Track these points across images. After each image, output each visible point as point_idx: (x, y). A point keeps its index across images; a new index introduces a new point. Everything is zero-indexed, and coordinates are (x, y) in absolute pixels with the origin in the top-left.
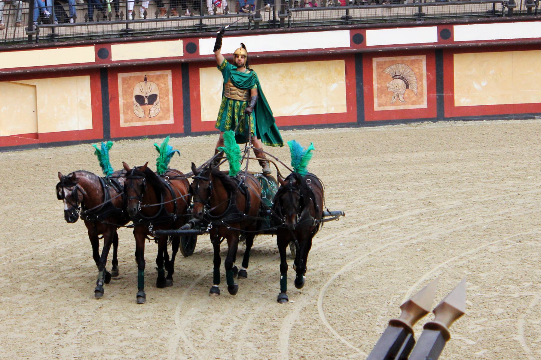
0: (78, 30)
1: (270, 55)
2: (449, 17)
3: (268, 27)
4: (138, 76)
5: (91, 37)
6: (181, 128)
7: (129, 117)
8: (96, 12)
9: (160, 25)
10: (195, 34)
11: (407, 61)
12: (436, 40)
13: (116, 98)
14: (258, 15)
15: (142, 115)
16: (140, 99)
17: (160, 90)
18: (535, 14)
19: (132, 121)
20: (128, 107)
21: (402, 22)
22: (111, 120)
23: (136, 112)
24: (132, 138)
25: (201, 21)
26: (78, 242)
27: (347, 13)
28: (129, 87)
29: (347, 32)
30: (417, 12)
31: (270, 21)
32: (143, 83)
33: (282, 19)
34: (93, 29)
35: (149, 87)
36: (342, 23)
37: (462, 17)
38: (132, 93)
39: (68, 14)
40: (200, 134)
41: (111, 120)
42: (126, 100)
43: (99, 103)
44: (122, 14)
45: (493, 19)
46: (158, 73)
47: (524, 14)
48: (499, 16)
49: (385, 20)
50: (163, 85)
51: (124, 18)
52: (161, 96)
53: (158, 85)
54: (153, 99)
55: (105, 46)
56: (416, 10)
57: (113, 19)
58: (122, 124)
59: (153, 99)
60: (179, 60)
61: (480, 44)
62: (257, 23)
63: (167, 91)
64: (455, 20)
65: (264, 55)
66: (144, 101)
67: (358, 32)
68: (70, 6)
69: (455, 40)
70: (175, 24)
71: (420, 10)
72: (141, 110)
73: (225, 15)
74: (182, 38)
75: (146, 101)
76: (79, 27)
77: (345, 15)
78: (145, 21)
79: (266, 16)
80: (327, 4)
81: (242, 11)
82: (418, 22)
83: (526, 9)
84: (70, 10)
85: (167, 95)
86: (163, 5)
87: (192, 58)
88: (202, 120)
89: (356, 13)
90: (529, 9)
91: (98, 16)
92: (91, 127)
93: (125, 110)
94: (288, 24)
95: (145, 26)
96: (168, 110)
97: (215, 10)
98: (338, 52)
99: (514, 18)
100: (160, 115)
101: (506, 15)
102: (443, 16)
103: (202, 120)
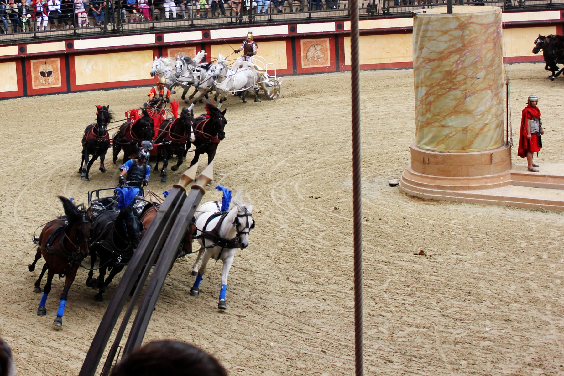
0: (8, 37)
1: (112, 48)
2: (208, 26)
3: (111, 33)
5: (16, 41)
6: (65, 89)
7: (37, 84)
8: (18, 28)
9: (53, 33)
10: (72, 38)
11: (186, 50)
12: (201, 38)
13: (30, 73)
14: (105, 27)
15: (44, 82)
16: (43, 74)
17: (54, 69)
18: (254, 23)
19: (39, 86)
20: (37, 78)
21: (183, 29)
22: (28, 85)
23: (41, 81)
24: (39, 95)
25: (75, 31)
26: (11, 151)
27: (153, 25)
28: (37, 67)
29: (154, 35)
30: (191, 23)
31: (112, 30)
33: (119, 29)
34: (16, 36)
36: (150, 30)
37: (215, 26)
38: (39, 70)
39: (4, 29)
40: (76, 92)
41: (28, 85)
42: (35, 74)
43: (21, 77)
44: (32, 28)
45: (231, 26)
46: (53, 59)
47: (248, 23)
48: (234, 25)
49: (174, 28)
50: (55, 66)
51: (33, 31)
53: (52, 66)
54: (50, 73)
55: (23, 46)
56: (190, 22)
57: (28, 30)
58: (34, 87)
59: (50, 73)
60: (63, 52)
61: (225, 40)
62: (105, 31)
63: (57, 69)
64: (211, 27)
65: (109, 48)
67: (159, 35)
68: (5, 25)
69: (212, 38)
70: (61, 33)
71: (192, 22)
73: (87, 28)
74: (65, 40)
75: (46, 75)
76: (9, 36)
77: (152, 26)
78: (44, 32)
79: (109, 27)
80: (142, 20)
81: (97, 25)
82: (191, 29)
83: (249, 20)
84: (5, 27)
85: (57, 71)
86: (54, 23)
87: (70, 51)
88: (77, 84)
89: (158, 25)
90: (250, 20)
91: (19, 30)
92: (17, 90)
94: (122, 32)
95: (45, 34)
96: (58, 79)
97: (82, 25)
98: (149, 46)
99: (242, 25)
100: (54, 82)
101: (238, 24)
102: (204, 26)
103: (77, 84)
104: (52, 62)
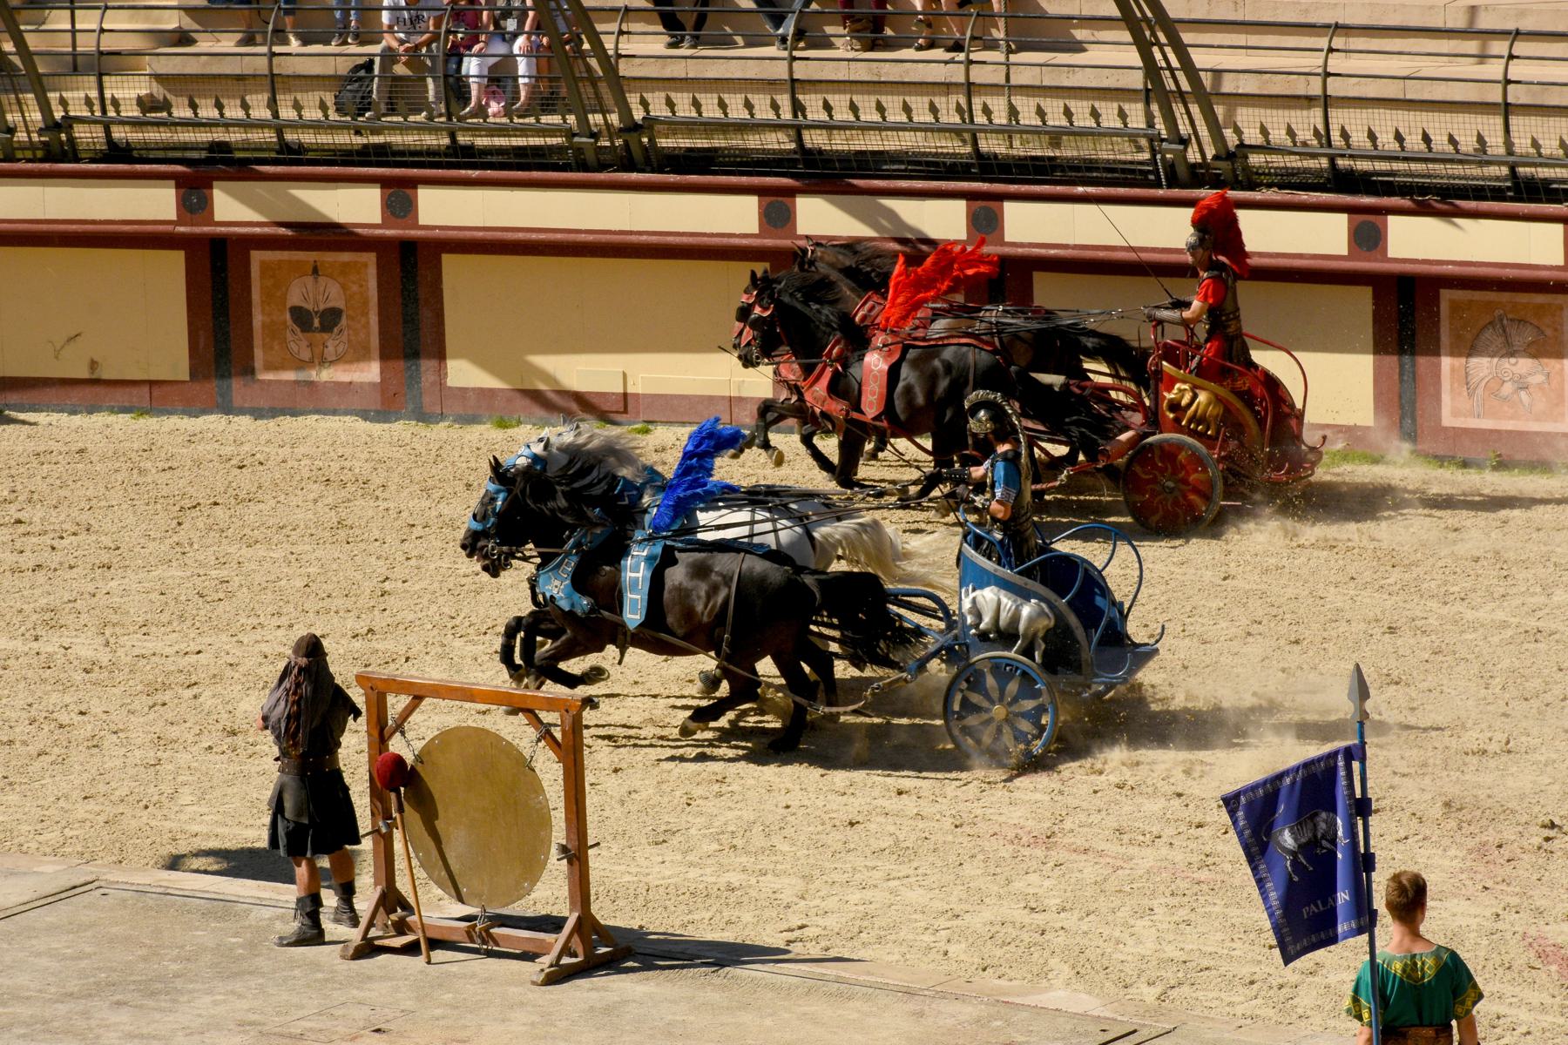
4: (298, 262)
15: (306, 354)
16: (301, 317)
20: (273, 331)
23: (292, 345)
32: (309, 280)
35: (322, 289)
38: (284, 298)
50: (355, 288)
52: (350, 312)
53: (344, 287)
63: (366, 303)
66: (312, 324)
72: (304, 343)
75: (316, 323)
85: (365, 314)
93: (268, 340)
104: (345, 268)
